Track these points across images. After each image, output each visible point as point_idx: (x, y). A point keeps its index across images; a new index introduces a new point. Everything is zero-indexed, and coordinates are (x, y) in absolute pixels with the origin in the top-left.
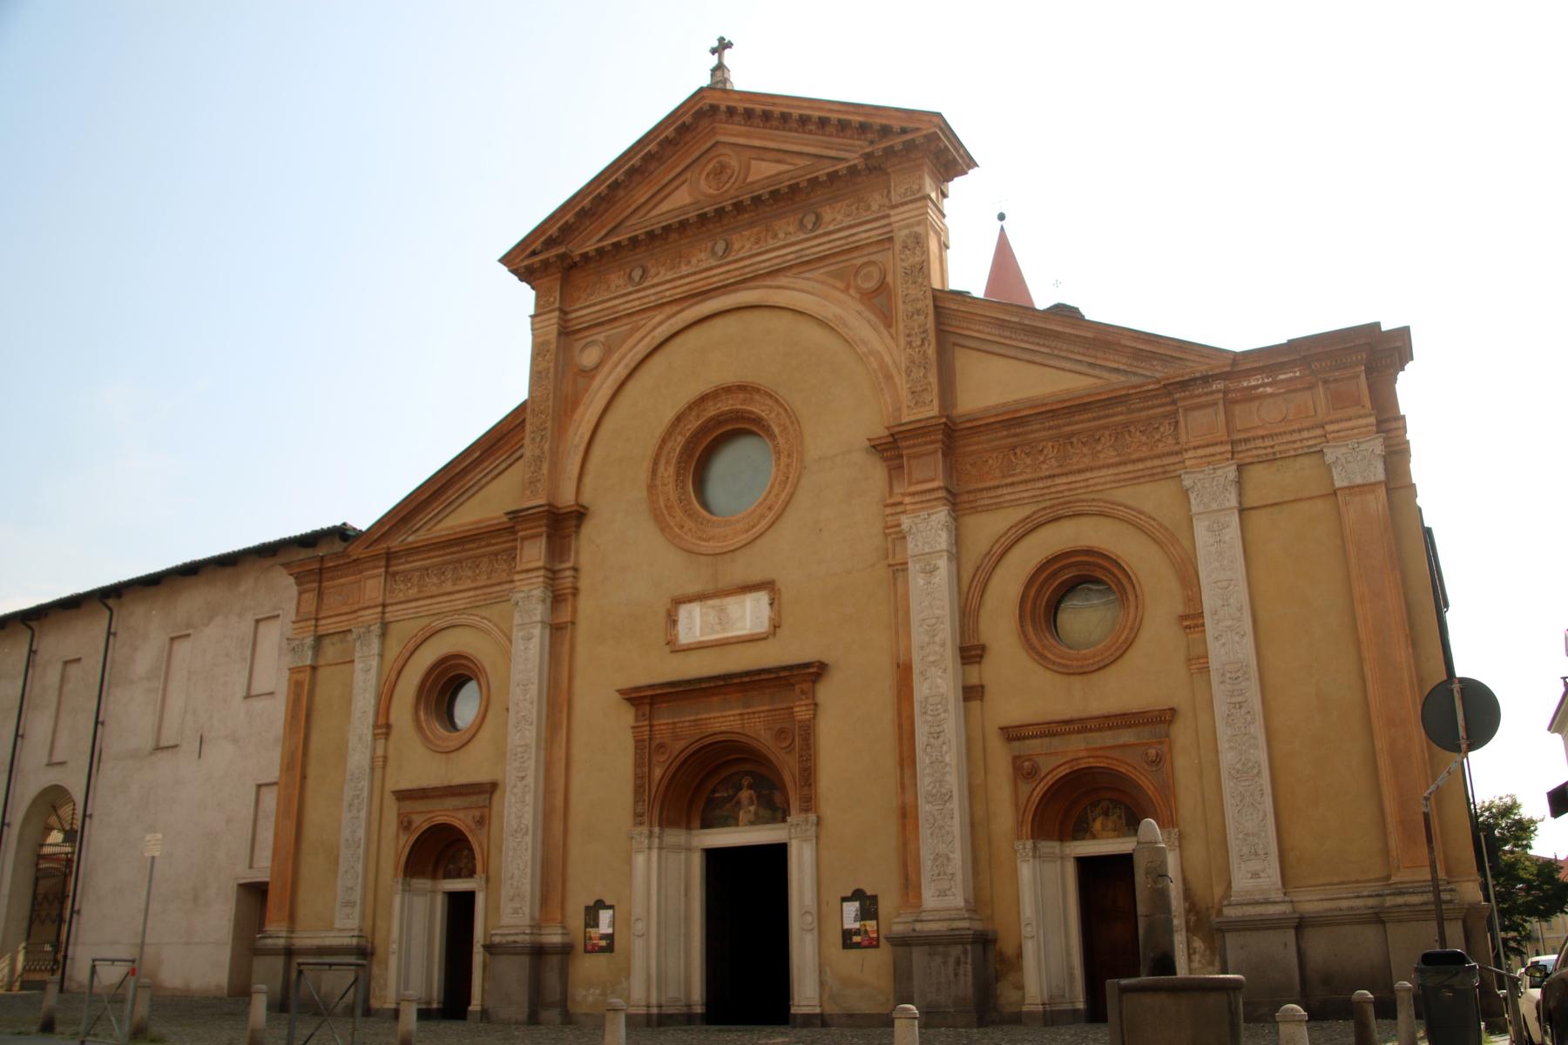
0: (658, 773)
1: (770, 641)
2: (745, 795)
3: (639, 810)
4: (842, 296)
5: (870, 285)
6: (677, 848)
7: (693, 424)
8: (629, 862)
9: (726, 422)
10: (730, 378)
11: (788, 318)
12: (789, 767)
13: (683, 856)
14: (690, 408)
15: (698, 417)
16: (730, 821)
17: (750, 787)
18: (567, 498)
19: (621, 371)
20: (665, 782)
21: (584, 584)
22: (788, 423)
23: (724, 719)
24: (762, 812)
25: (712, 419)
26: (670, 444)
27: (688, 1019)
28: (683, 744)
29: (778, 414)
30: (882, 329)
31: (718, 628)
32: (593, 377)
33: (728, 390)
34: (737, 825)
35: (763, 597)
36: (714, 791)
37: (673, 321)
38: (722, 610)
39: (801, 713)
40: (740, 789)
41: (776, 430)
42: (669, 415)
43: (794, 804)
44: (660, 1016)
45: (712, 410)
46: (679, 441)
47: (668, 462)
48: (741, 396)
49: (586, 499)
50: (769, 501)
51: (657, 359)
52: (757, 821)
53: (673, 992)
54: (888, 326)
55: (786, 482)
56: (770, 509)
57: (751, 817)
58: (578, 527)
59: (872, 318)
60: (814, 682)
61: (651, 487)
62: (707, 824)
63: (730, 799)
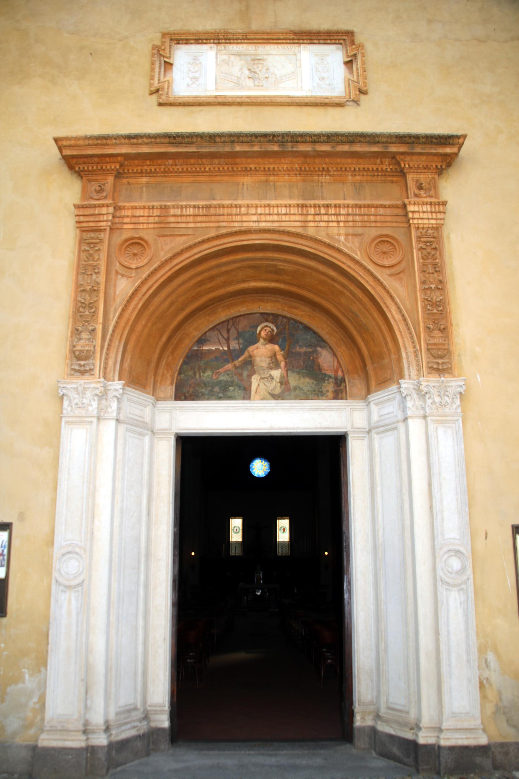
0: (124, 287)
1: (350, 110)
2: (262, 351)
3: (82, 345)
12: (401, 296)
13: (147, 439)
16: (234, 388)
17: (271, 339)
20: (138, 303)
23: (264, 210)
24: (294, 380)
28: (180, 243)
31: (250, 83)
35: (334, 56)
36: (201, 341)
39: (420, 214)
40: (254, 340)
43: (410, 353)
52: (285, 393)
53: (126, 697)
57: (275, 386)
60: (440, 172)
62: (185, 392)
63: (231, 355)
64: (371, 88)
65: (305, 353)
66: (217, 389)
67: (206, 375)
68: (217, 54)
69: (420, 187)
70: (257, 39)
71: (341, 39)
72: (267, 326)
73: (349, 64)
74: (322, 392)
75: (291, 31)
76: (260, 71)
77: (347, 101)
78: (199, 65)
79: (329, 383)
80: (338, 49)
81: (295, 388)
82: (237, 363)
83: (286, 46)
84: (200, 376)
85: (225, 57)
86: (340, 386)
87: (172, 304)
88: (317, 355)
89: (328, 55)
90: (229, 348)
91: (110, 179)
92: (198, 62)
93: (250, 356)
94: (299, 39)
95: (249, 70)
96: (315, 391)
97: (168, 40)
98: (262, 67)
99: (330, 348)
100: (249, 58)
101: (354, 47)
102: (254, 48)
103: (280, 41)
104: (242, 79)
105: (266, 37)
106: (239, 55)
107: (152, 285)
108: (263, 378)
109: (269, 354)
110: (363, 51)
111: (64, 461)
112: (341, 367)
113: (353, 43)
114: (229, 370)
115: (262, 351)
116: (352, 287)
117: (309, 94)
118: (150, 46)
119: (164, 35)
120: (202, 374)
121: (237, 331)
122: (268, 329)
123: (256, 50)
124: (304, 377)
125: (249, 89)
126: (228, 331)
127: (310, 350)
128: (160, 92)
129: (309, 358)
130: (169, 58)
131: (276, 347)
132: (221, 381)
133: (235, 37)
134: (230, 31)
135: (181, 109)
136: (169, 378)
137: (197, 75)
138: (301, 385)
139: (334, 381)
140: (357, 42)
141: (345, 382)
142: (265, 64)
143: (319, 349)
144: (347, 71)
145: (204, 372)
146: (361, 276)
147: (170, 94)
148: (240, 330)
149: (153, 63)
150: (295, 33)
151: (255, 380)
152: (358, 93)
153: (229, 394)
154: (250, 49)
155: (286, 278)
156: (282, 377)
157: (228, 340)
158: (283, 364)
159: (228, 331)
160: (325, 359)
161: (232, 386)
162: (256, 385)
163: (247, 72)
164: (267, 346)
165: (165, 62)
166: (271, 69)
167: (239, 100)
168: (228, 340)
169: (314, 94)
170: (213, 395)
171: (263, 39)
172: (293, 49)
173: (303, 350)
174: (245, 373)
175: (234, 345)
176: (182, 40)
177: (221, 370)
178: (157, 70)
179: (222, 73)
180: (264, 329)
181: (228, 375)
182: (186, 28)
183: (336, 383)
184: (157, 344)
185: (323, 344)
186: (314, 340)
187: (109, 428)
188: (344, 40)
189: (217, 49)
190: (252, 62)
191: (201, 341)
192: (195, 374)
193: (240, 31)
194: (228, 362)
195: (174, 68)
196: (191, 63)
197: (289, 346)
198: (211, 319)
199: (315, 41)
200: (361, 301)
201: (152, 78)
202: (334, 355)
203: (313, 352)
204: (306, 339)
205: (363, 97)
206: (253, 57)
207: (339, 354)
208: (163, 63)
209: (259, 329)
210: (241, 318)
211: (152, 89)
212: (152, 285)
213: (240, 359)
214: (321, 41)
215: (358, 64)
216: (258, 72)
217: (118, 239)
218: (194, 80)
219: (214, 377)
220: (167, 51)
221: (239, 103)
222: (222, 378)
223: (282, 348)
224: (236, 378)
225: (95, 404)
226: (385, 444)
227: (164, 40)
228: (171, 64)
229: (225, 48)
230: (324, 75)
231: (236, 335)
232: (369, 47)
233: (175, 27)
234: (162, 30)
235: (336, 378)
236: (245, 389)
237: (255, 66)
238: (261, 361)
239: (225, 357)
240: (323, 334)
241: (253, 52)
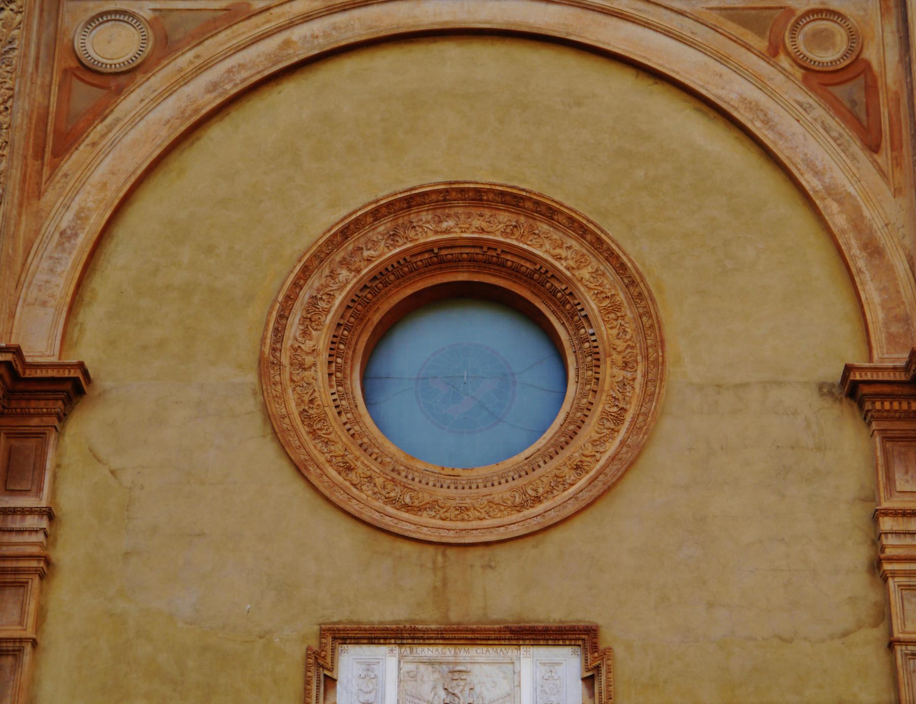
4: (762, 66)
5: (827, 57)
7: (381, 251)
9: (455, 263)
10: (481, 171)
11: (623, 82)
14: (377, 213)
15: (393, 236)
18: (40, 345)
19: (199, 94)
21: (66, 555)
22: (621, 297)
25: (428, 248)
26: (315, 282)
29: (596, 273)
30: (856, 147)
32: (119, 92)
33: (478, 197)
37: (340, 18)
38: (456, 673)
41: (593, 306)
42: (326, 219)
45: (428, 230)
46: (349, 280)
47: (310, 321)
48: (505, 217)
49: (86, 353)
50: (363, 464)
51: (289, 89)
54: (873, 148)
55: (618, 419)
56: (579, 468)
58: (62, 418)
59: (834, 123)
61: (266, 366)
68: (399, 662)
70: (458, 639)
71: (579, 639)
73: (589, 681)
75: (507, 627)
76: (461, 692)
78: (374, 681)
80: (574, 652)
83: (499, 648)
85: (411, 667)
89: (559, 664)
92: (372, 676)
94: (518, 639)
98: (464, 686)
100: (445, 668)
101: (596, 655)
102: (453, 652)
103: (490, 642)
105: (470, 636)
106: (431, 663)
110: (610, 662)
113: (595, 648)
118: (304, 647)
123: (455, 655)
130: (331, 670)
133: (426, 636)
134: (420, 627)
140: (602, 646)
142: (468, 678)
144: (586, 692)
149: (308, 682)
150: (512, 631)
154: (448, 653)
163: (443, 694)
165: (325, 675)
166: (478, 689)
171: (466, 639)
172: (510, 653)
176: (350, 638)
178: (314, 693)
179: (407, 694)
182: (355, 619)
189: (400, 654)
190: (450, 675)
193: (433, 627)
195: (338, 686)
196: (363, 676)
199: (542, 642)
214: (550, 642)
215: (601, 684)
216: (459, 695)
220: (329, 660)
228: (334, 681)
229: (411, 650)
232: (619, 652)
233: (340, 615)
234: (321, 621)
237: (455, 683)
241: (452, 659)
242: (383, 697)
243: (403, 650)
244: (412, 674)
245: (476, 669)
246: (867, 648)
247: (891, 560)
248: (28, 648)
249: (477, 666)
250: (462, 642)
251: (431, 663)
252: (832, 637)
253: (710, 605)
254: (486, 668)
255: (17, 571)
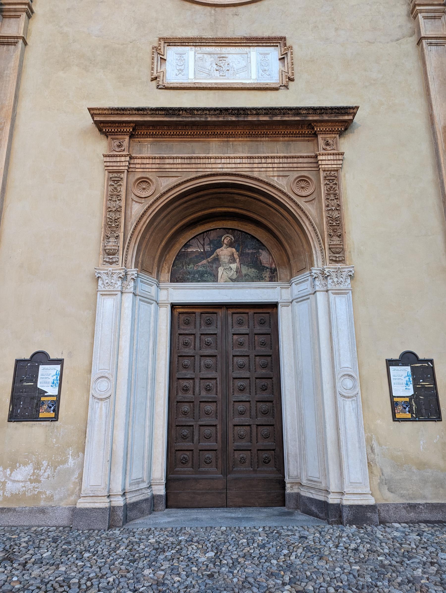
0: (137, 209)
2: (225, 252)
6: (147, 300)
8: (94, 309)
16: (208, 276)
17: (231, 245)
20: (147, 220)
23: (227, 160)
24: (244, 270)
27: (152, 503)
28: (172, 181)
31: (217, 74)
34: (215, 278)
36: (187, 245)
38: (222, 58)
39: (327, 162)
40: (219, 245)
44: (127, 507)
52: (240, 278)
53: (137, 473)
60: (341, 134)
63: (205, 255)
64: (296, 77)
65: (252, 253)
66: (197, 276)
67: (190, 267)
68: (195, 53)
69: (327, 144)
72: (228, 237)
74: (262, 277)
77: (280, 86)
79: (266, 272)
81: (245, 275)
82: (209, 259)
84: (186, 268)
85: (201, 55)
86: (274, 273)
87: (168, 221)
88: (259, 254)
90: (204, 250)
91: (127, 138)
93: (217, 255)
95: (216, 64)
96: (258, 277)
97: (162, 42)
98: (225, 63)
99: (268, 250)
101: (286, 47)
102: (219, 49)
104: (212, 71)
107: (155, 209)
108: (226, 269)
109: (229, 254)
110: (292, 51)
111: (99, 319)
112: (274, 262)
113: (285, 45)
114: (205, 264)
115: (225, 252)
116: (282, 210)
117: (256, 82)
119: (160, 39)
120: (187, 266)
121: (209, 239)
122: (229, 238)
124: (251, 268)
125: (217, 78)
126: (204, 239)
127: (255, 251)
128: (158, 79)
129: (254, 256)
131: (234, 250)
132: (199, 271)
135: (172, 91)
136: (167, 269)
137: (182, 68)
138: (249, 273)
139: (269, 270)
141: (276, 271)
143: (260, 250)
144: (281, 65)
145: (189, 265)
146: (287, 203)
147: (164, 81)
148: (211, 239)
150: (247, 39)
151: (220, 270)
152: (288, 80)
153: (204, 279)
154: (217, 50)
155: (240, 205)
156: (237, 268)
157: (203, 245)
158: (238, 260)
159: (204, 239)
160: (264, 257)
161: (206, 274)
162: (221, 273)
163: (215, 66)
164: (228, 249)
165: (161, 58)
166: (231, 64)
167: (210, 86)
168: (203, 245)
169: (259, 82)
170: (194, 280)
172: (246, 50)
173: (250, 251)
174: (214, 266)
175: (207, 248)
177: (200, 264)
178: (155, 64)
180: (226, 239)
181: (204, 267)
183: (271, 272)
184: (159, 246)
185: (263, 247)
186: (257, 245)
187: (128, 299)
188: (280, 43)
190: (218, 59)
191: (187, 245)
192: (183, 266)
194: (204, 259)
195: (167, 61)
197: (242, 249)
198: (193, 232)
200: (287, 219)
201: (152, 69)
202: (270, 254)
203: (256, 252)
204: (253, 244)
205: (291, 83)
206: (219, 56)
207: (273, 254)
208: (159, 58)
209: (223, 238)
210: (212, 231)
211: (152, 77)
212: (155, 209)
213: (211, 257)
215: (288, 59)
216: (223, 66)
217: (133, 178)
218: (180, 72)
219: (195, 268)
220: (162, 50)
221: (210, 88)
222: (200, 269)
223: (237, 251)
224: (208, 269)
225: (119, 283)
226: (302, 308)
227: (160, 42)
228: (165, 60)
230: (266, 68)
231: (209, 242)
235: (271, 269)
236: (214, 276)
237: (221, 62)
238: (225, 258)
239: (202, 256)
240: (263, 241)
241: (219, 52)
242: (188, 67)
243: (196, 48)
244: (201, 58)
245: (230, 56)
246: (409, 44)
247: (419, 5)
248: (21, 41)
249: (231, 55)
250: (224, 44)
251: (209, 54)
252: (392, 41)
253: (336, 29)
254: (235, 56)
255: (15, 10)
